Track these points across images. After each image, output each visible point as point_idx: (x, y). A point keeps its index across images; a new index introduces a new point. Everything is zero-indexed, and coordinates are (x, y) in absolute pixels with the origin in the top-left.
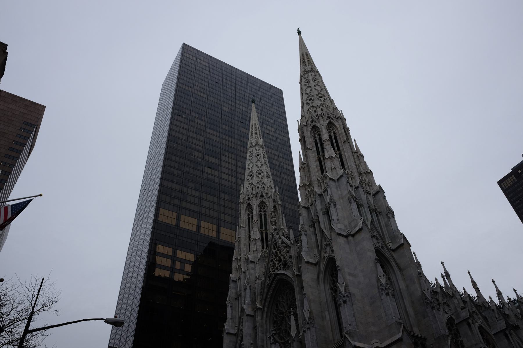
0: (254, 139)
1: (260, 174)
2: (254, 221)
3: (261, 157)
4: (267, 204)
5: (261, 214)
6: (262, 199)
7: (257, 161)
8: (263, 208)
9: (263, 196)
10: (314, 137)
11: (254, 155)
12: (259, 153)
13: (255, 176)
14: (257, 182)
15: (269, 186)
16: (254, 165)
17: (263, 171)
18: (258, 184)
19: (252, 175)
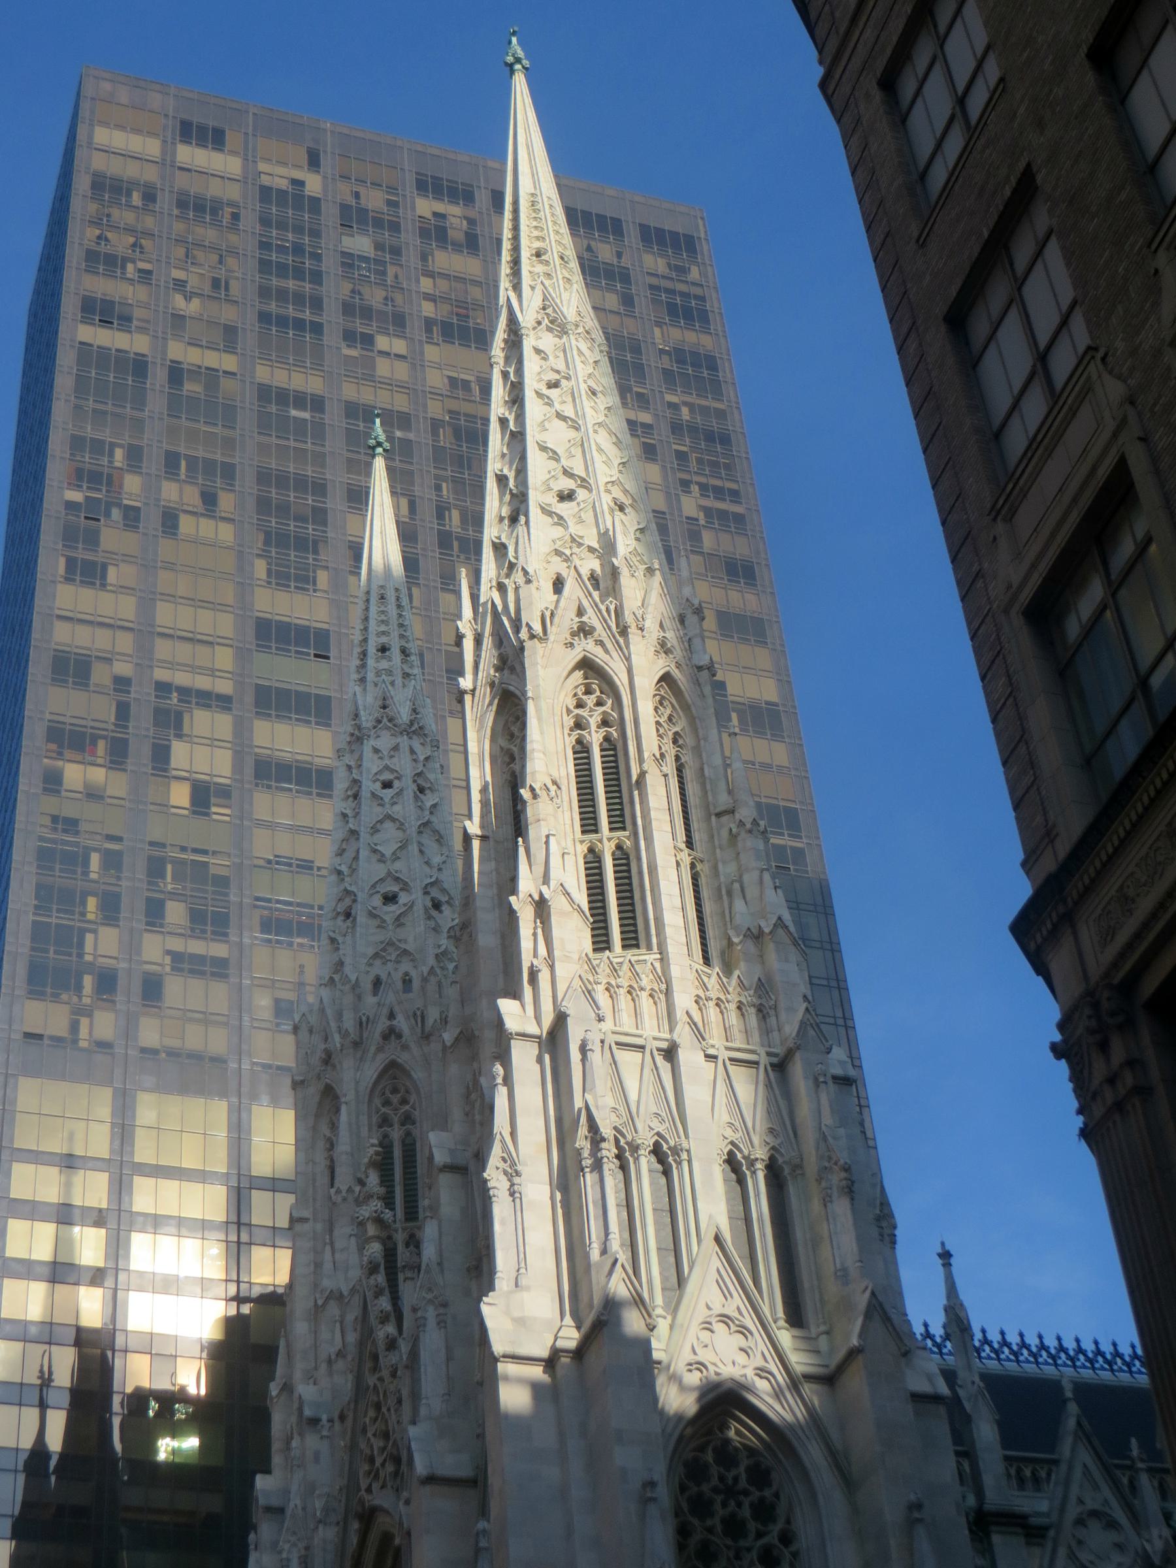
0: (370, 686)
1: (390, 899)
2: (338, 1191)
3: (400, 793)
4: (418, 1074)
5: (385, 1136)
6: (392, 1052)
7: (381, 822)
8: (395, 1099)
9: (399, 1036)
10: (507, 759)
11: (369, 786)
12: (393, 771)
13: (362, 918)
14: (371, 951)
15: (425, 974)
16: (364, 854)
17: (406, 884)
18: (378, 962)
19: (350, 907)
